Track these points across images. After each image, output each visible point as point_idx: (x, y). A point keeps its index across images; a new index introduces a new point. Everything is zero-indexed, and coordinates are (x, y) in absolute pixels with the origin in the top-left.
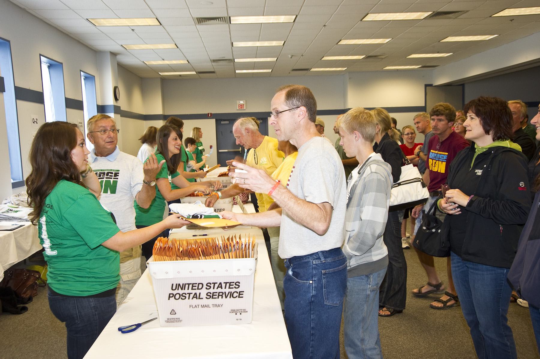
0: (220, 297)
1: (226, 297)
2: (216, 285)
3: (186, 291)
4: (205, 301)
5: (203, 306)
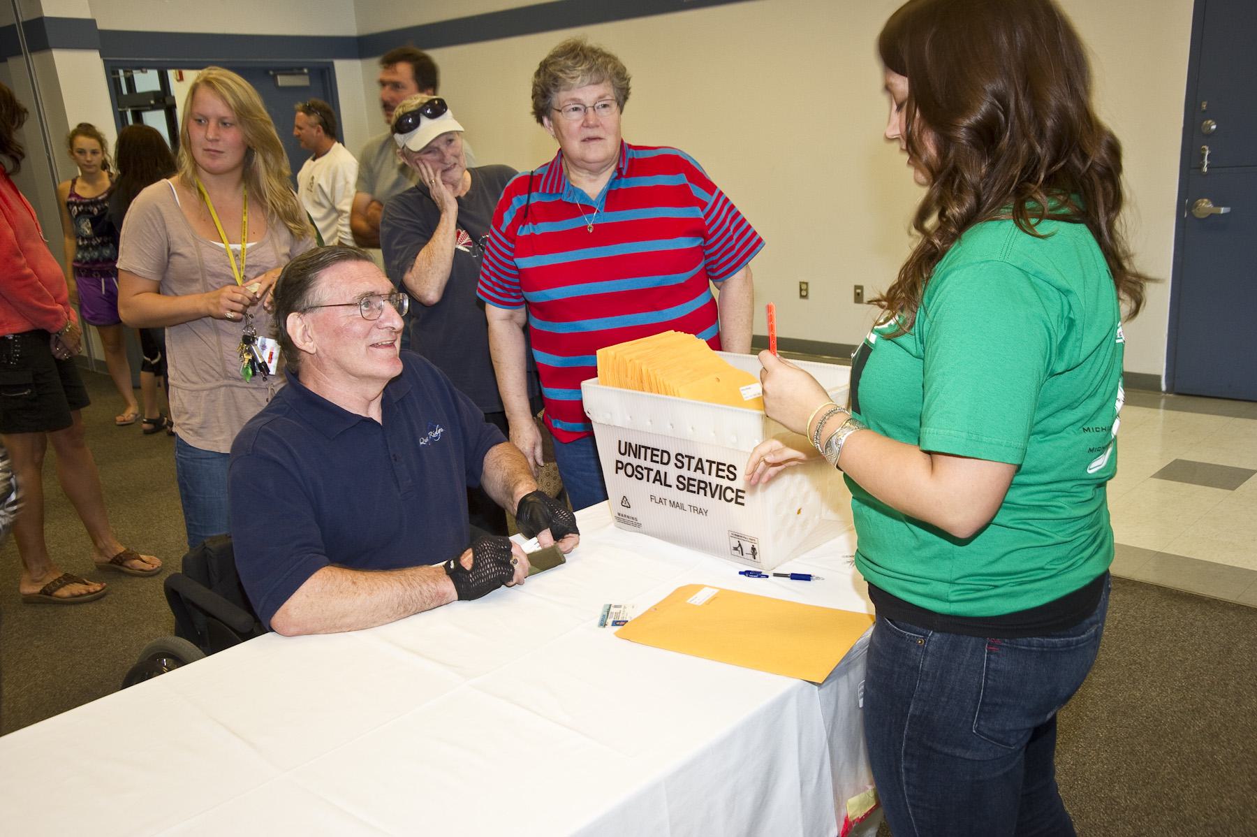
0: (702, 492)
2: (694, 463)
3: (641, 462)
4: (674, 494)
5: (674, 505)
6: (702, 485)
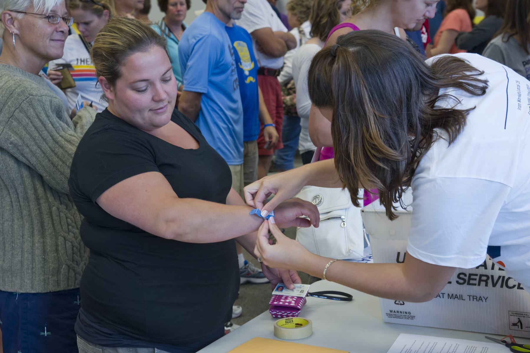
0: (483, 284)
1: (494, 285)
5: (451, 297)
6: (484, 278)
